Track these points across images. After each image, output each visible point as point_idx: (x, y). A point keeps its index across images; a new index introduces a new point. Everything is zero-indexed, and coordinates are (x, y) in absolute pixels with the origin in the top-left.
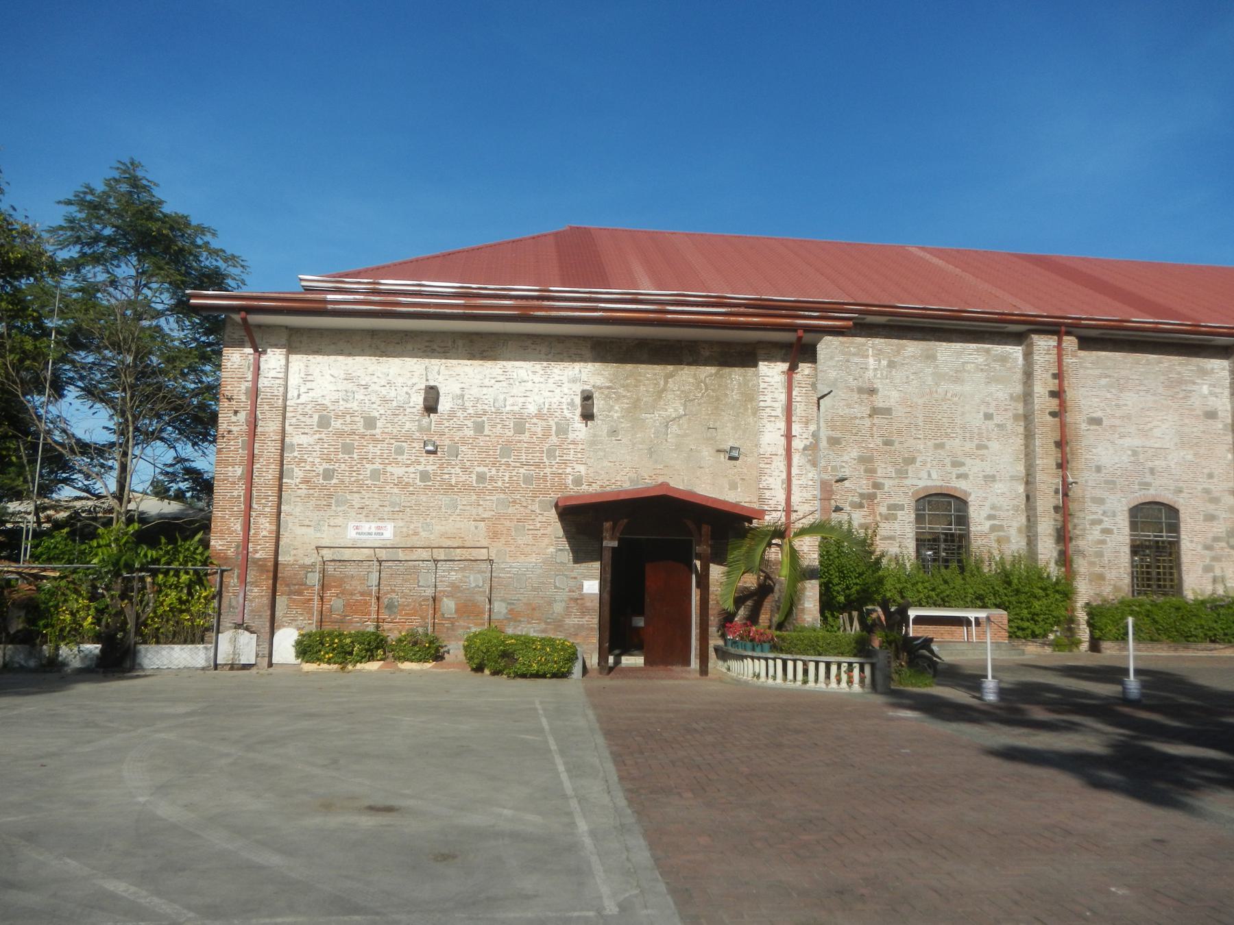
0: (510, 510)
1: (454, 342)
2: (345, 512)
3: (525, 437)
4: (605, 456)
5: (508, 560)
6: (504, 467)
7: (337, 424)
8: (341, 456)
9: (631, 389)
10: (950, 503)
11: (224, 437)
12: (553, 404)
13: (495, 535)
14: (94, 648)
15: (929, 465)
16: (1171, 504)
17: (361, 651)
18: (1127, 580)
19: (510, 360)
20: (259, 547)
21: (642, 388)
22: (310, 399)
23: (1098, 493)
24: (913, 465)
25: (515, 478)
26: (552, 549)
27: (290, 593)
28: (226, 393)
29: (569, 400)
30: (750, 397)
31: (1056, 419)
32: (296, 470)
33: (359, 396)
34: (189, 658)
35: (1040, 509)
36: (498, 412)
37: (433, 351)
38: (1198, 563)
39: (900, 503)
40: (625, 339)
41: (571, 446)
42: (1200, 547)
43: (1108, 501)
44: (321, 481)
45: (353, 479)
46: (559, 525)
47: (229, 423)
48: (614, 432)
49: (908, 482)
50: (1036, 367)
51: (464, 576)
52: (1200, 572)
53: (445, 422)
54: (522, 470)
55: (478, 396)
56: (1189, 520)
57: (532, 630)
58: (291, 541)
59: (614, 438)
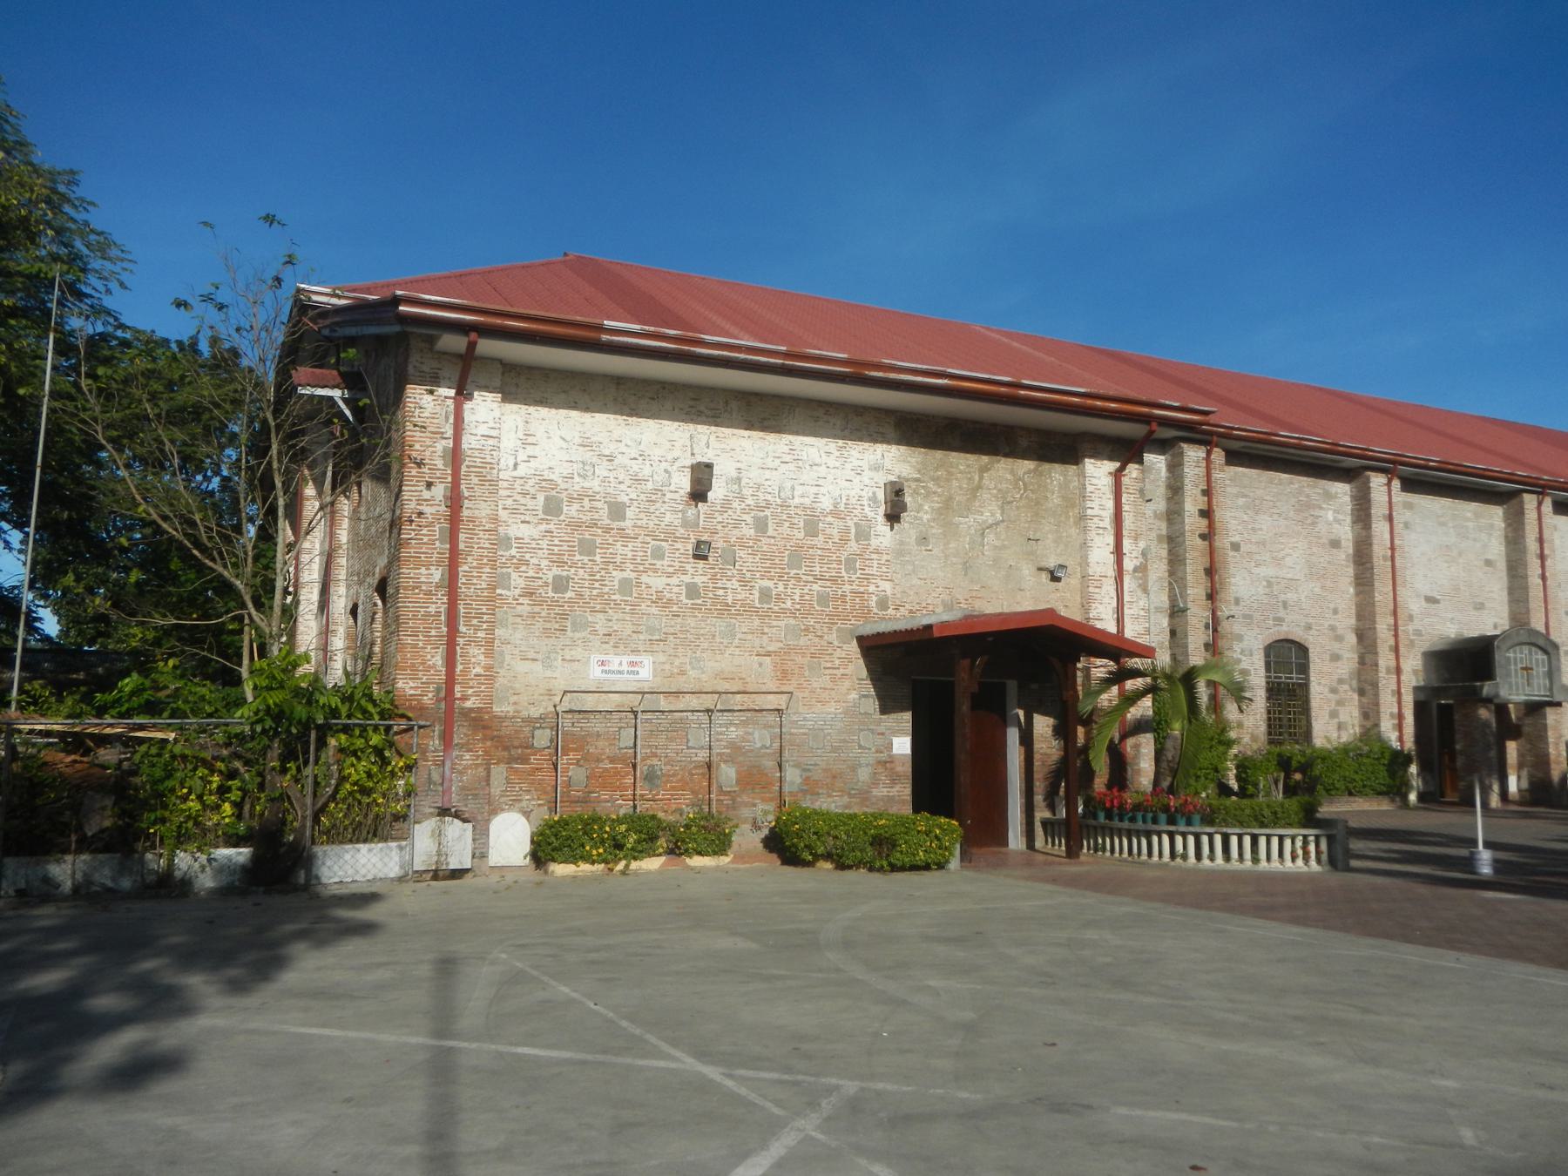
0: (803, 641)
1: (726, 403)
2: (585, 640)
3: (819, 541)
4: (914, 571)
5: (801, 710)
6: (793, 581)
7: (571, 511)
8: (578, 557)
9: (942, 484)
11: (412, 521)
12: (851, 498)
13: (784, 675)
14: (241, 854)
16: (1302, 642)
17: (639, 842)
18: (1263, 728)
19: (797, 433)
20: (470, 691)
21: (955, 484)
22: (533, 472)
25: (807, 597)
26: (854, 695)
27: (511, 760)
28: (414, 454)
29: (870, 494)
30: (1077, 500)
31: (1207, 543)
32: (514, 576)
33: (602, 471)
34: (379, 865)
35: (1191, 647)
36: (784, 506)
37: (700, 413)
40: (933, 417)
41: (874, 556)
42: (1327, 690)
43: (1246, 637)
44: (551, 594)
45: (595, 592)
46: (861, 662)
47: (420, 501)
48: (923, 539)
50: (1187, 481)
51: (746, 733)
52: (1327, 717)
53: (717, 514)
54: (815, 587)
55: (758, 481)
56: (1317, 660)
57: (831, 803)
58: (509, 681)
59: (923, 548)
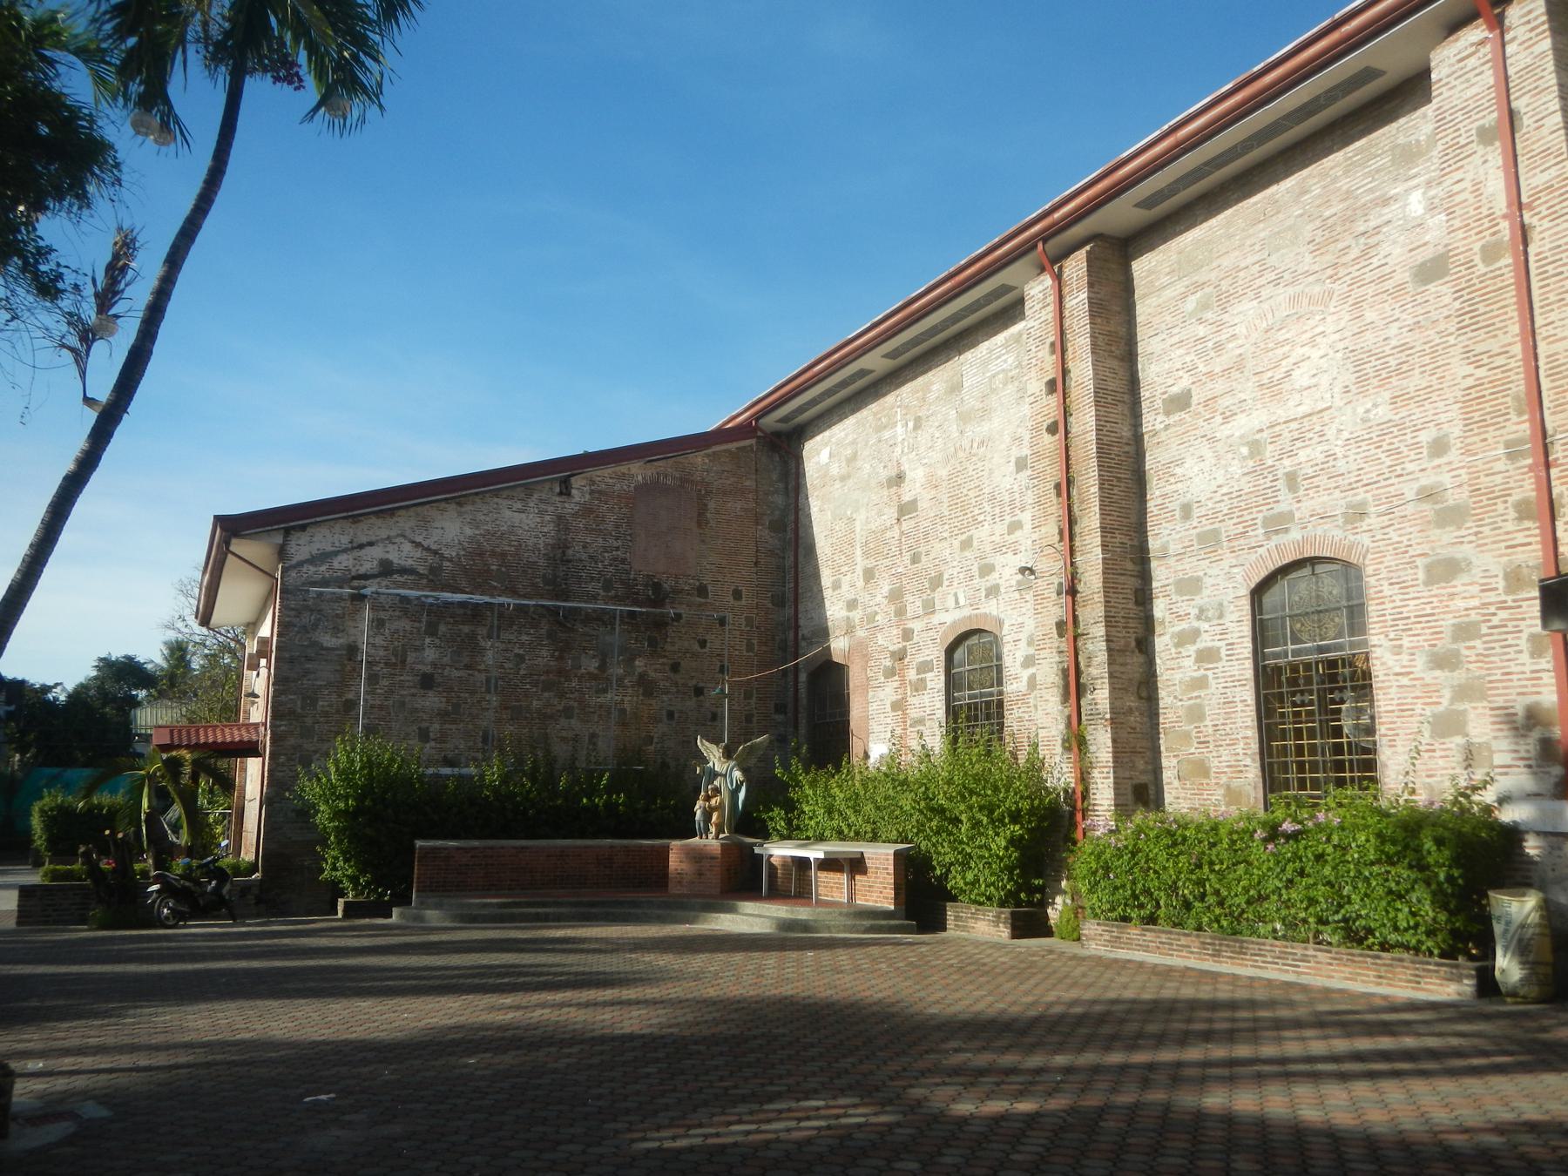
15: (955, 583)
23: (1189, 567)
24: (940, 589)
38: (1418, 709)
39: (929, 659)
42: (1420, 662)
43: (1206, 579)
49: (936, 619)
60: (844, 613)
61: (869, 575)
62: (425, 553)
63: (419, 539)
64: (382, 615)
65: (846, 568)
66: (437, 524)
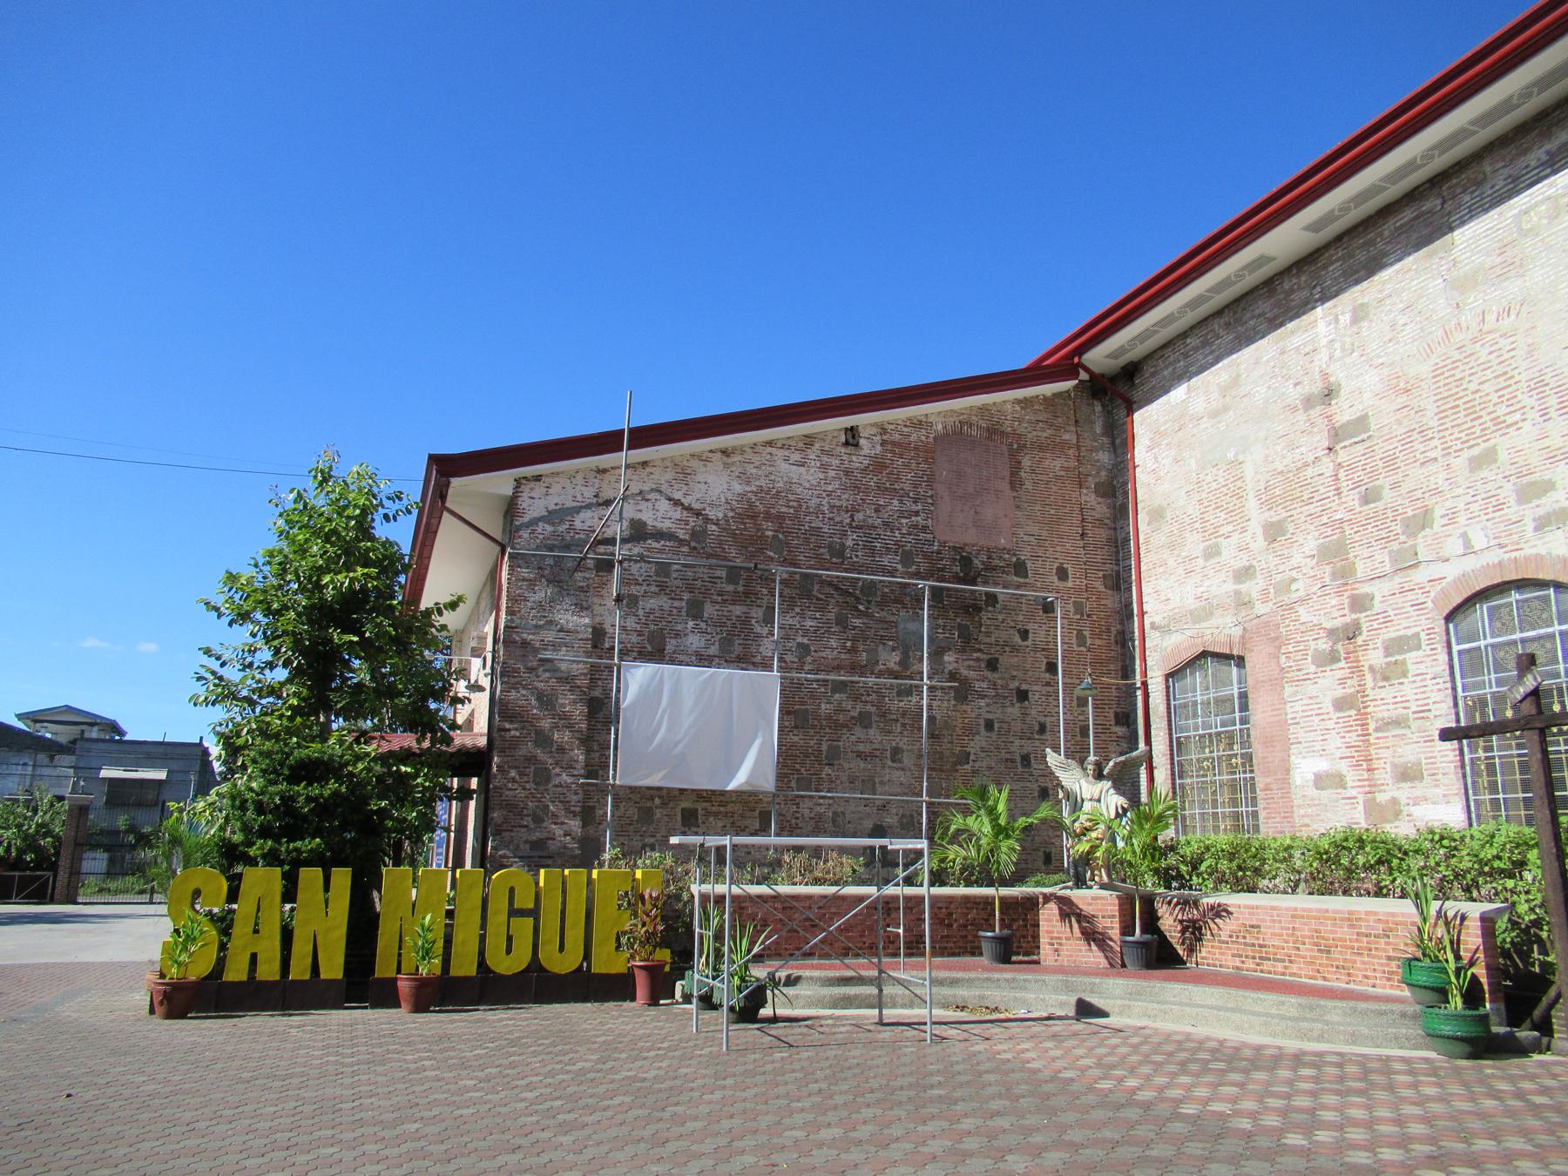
10: (1546, 599)
15: (1462, 519)
39: (1409, 632)
49: (1420, 576)
60: (1230, 586)
61: (1274, 532)
62: (685, 513)
63: (677, 495)
64: (634, 590)
65: (1230, 528)
66: (700, 478)
